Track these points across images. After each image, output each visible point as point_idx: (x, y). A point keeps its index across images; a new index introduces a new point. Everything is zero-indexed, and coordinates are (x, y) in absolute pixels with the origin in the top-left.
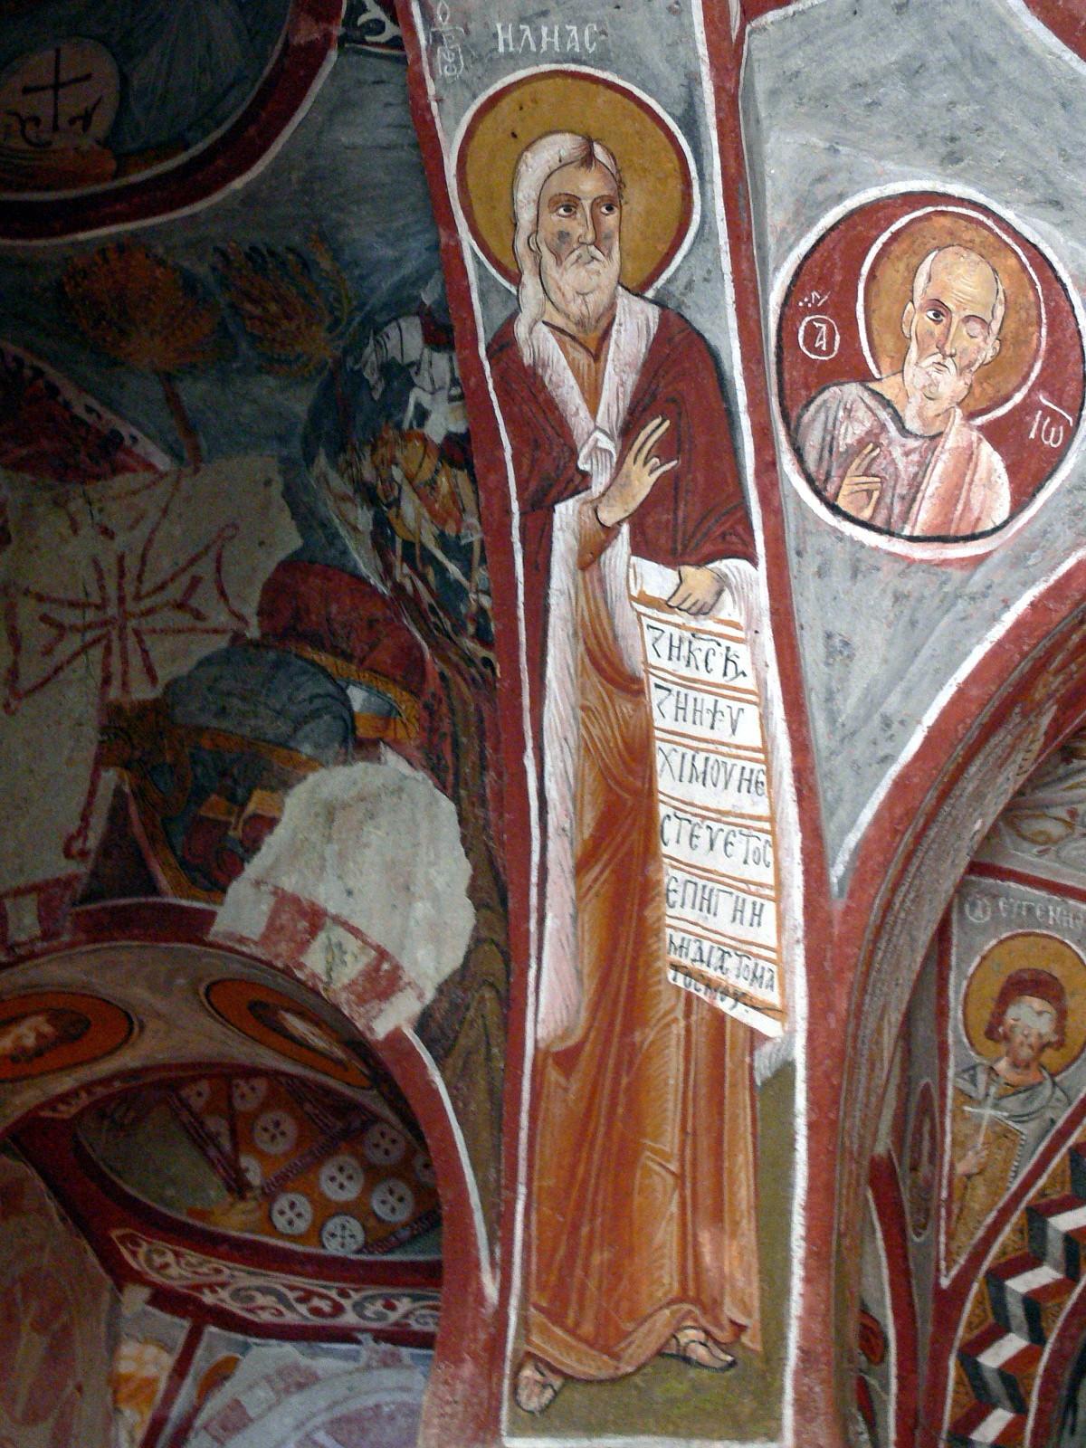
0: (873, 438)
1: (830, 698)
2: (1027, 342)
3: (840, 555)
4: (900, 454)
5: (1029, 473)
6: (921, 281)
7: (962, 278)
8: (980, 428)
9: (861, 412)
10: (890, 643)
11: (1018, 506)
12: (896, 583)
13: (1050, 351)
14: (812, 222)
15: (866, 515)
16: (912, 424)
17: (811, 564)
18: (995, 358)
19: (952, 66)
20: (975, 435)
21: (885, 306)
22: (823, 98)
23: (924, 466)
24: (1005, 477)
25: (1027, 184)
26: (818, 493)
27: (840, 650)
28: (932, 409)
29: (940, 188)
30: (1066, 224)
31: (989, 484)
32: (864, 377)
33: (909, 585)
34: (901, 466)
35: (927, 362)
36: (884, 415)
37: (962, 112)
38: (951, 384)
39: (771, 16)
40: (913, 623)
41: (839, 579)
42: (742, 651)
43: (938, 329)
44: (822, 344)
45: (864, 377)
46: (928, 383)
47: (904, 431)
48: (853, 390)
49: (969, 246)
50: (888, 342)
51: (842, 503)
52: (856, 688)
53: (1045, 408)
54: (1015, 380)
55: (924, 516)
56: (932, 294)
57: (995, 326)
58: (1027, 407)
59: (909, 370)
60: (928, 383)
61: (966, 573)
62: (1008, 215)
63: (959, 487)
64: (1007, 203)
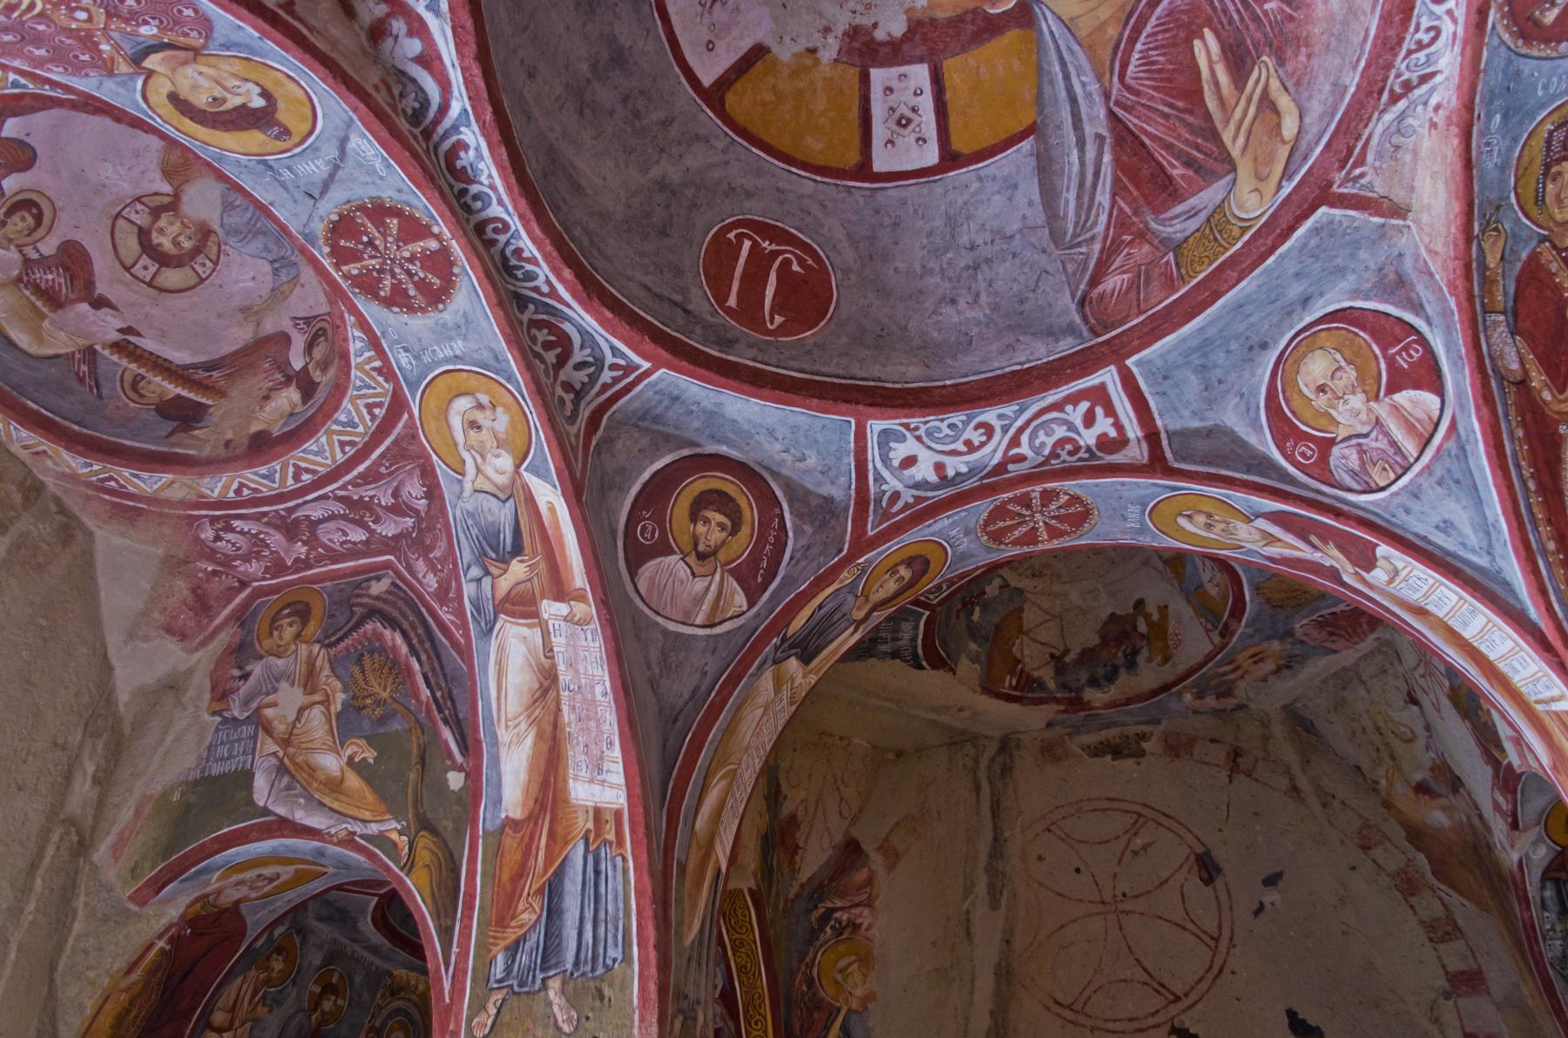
0: (1362, 451)
1: (1464, 545)
2: (1360, 348)
3: (1403, 499)
4: (1376, 443)
5: (1428, 376)
6: (1305, 391)
7: (1317, 367)
8: (1386, 395)
9: (1347, 452)
10: (1458, 501)
11: (1439, 390)
12: (1432, 480)
13: (1372, 335)
14: (1261, 426)
15: (1392, 476)
16: (1365, 430)
17: (1401, 515)
18: (1357, 369)
19: (1204, 355)
20: (1387, 400)
21: (1307, 414)
22: (1210, 402)
23: (1387, 434)
24: (1418, 392)
25: (1290, 314)
26: (1372, 491)
27: (1446, 527)
28: (1363, 416)
29: (1277, 353)
30: (1321, 295)
31: (1415, 403)
32: (1332, 442)
33: (1439, 471)
34: (1378, 445)
35: (1341, 407)
36: (1354, 442)
37: (1234, 346)
38: (1357, 401)
39: (1159, 423)
40: (1458, 482)
41: (1416, 506)
42: (1415, 572)
43: (1329, 395)
44: (1309, 453)
45: (1332, 442)
46: (1351, 412)
47: (1366, 436)
48: (1336, 451)
49: (1305, 356)
50: (1322, 422)
51: (1382, 484)
52: (1468, 530)
53: (1399, 353)
54: (1373, 364)
55: (1410, 447)
56: (1313, 388)
57: (1343, 363)
58: (1391, 362)
59: (1340, 419)
60: (1351, 412)
61: (1454, 438)
62: (1308, 320)
63: (1407, 421)
64: (1301, 320)
